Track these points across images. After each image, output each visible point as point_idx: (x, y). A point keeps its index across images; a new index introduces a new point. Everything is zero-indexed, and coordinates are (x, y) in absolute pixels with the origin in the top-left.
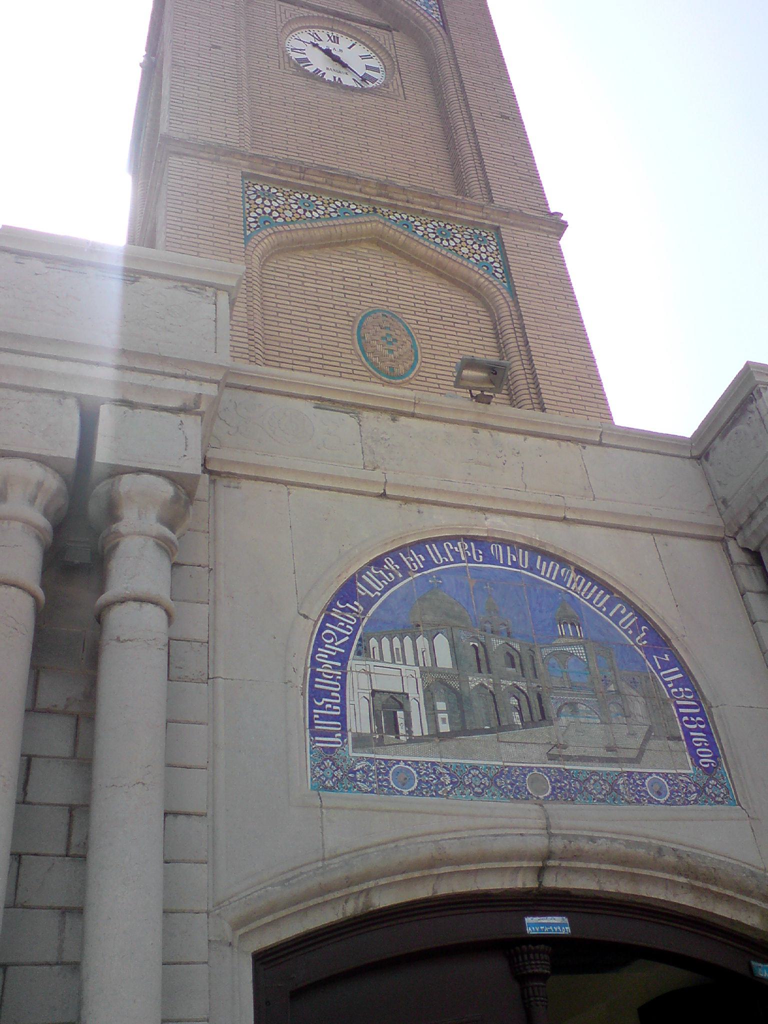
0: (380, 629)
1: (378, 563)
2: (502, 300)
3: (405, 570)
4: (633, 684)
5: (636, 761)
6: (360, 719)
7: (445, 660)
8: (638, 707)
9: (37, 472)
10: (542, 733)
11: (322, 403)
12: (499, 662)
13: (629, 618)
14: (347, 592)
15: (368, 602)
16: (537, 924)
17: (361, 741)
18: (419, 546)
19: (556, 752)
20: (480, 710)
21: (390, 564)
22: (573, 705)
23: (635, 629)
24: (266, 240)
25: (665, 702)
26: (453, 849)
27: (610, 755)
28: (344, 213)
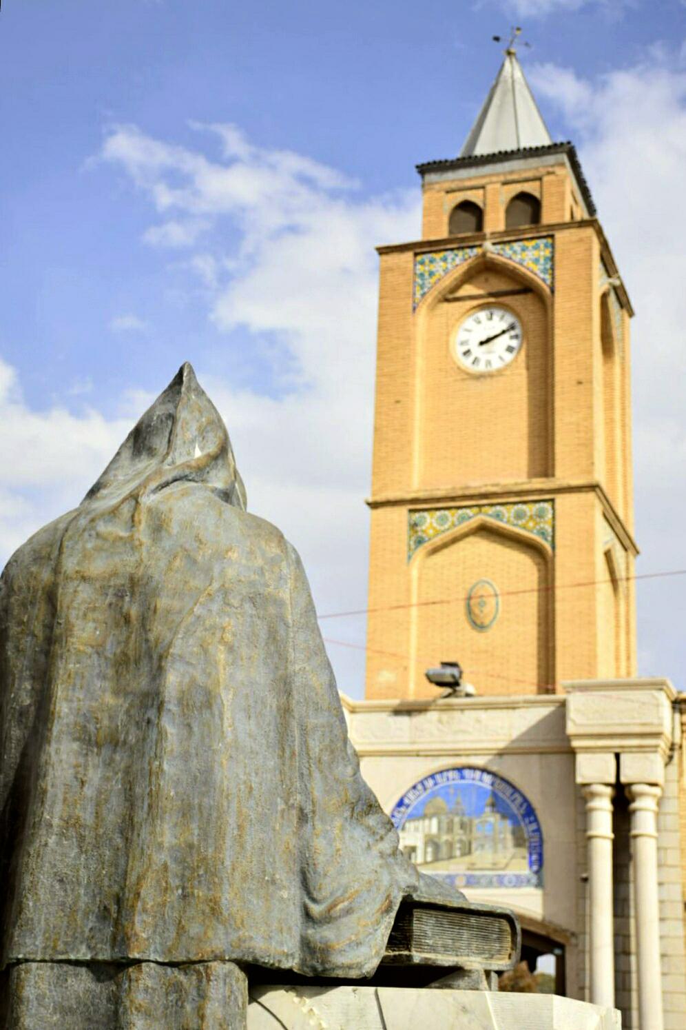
0: (412, 818)
1: (414, 787)
3: (425, 789)
5: (503, 869)
7: (434, 830)
10: (467, 859)
12: (457, 827)
13: (520, 800)
15: (408, 806)
18: (432, 776)
19: (472, 867)
20: (444, 851)
21: (420, 787)
22: (482, 846)
23: (521, 805)
24: (421, 552)
25: (524, 841)
27: (494, 867)
28: (462, 519)
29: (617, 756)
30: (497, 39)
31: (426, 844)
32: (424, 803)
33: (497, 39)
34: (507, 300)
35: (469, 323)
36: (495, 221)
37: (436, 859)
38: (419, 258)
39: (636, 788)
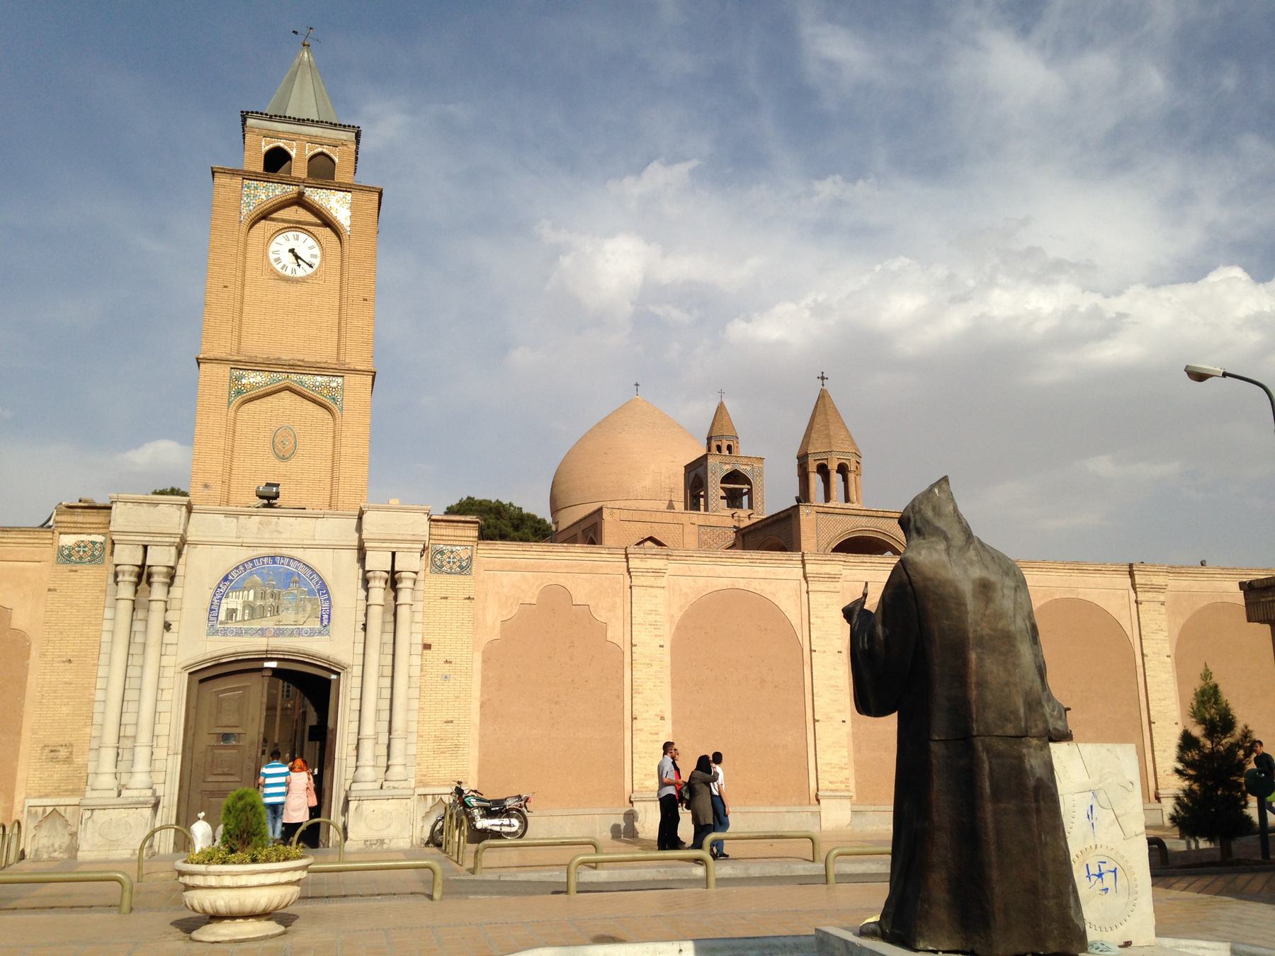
0: (234, 589)
1: (237, 568)
2: (338, 414)
4: (310, 600)
6: (222, 616)
7: (251, 598)
8: (309, 608)
9: (131, 568)
10: (275, 618)
11: (227, 515)
12: (268, 596)
14: (226, 579)
16: (267, 664)
17: (221, 623)
18: (252, 561)
26: (239, 650)
29: (394, 554)
30: (295, 32)
31: (244, 608)
32: (244, 579)
33: (295, 32)
34: (311, 228)
35: (280, 239)
36: (299, 168)
37: (252, 617)
38: (246, 182)
39: (403, 574)
